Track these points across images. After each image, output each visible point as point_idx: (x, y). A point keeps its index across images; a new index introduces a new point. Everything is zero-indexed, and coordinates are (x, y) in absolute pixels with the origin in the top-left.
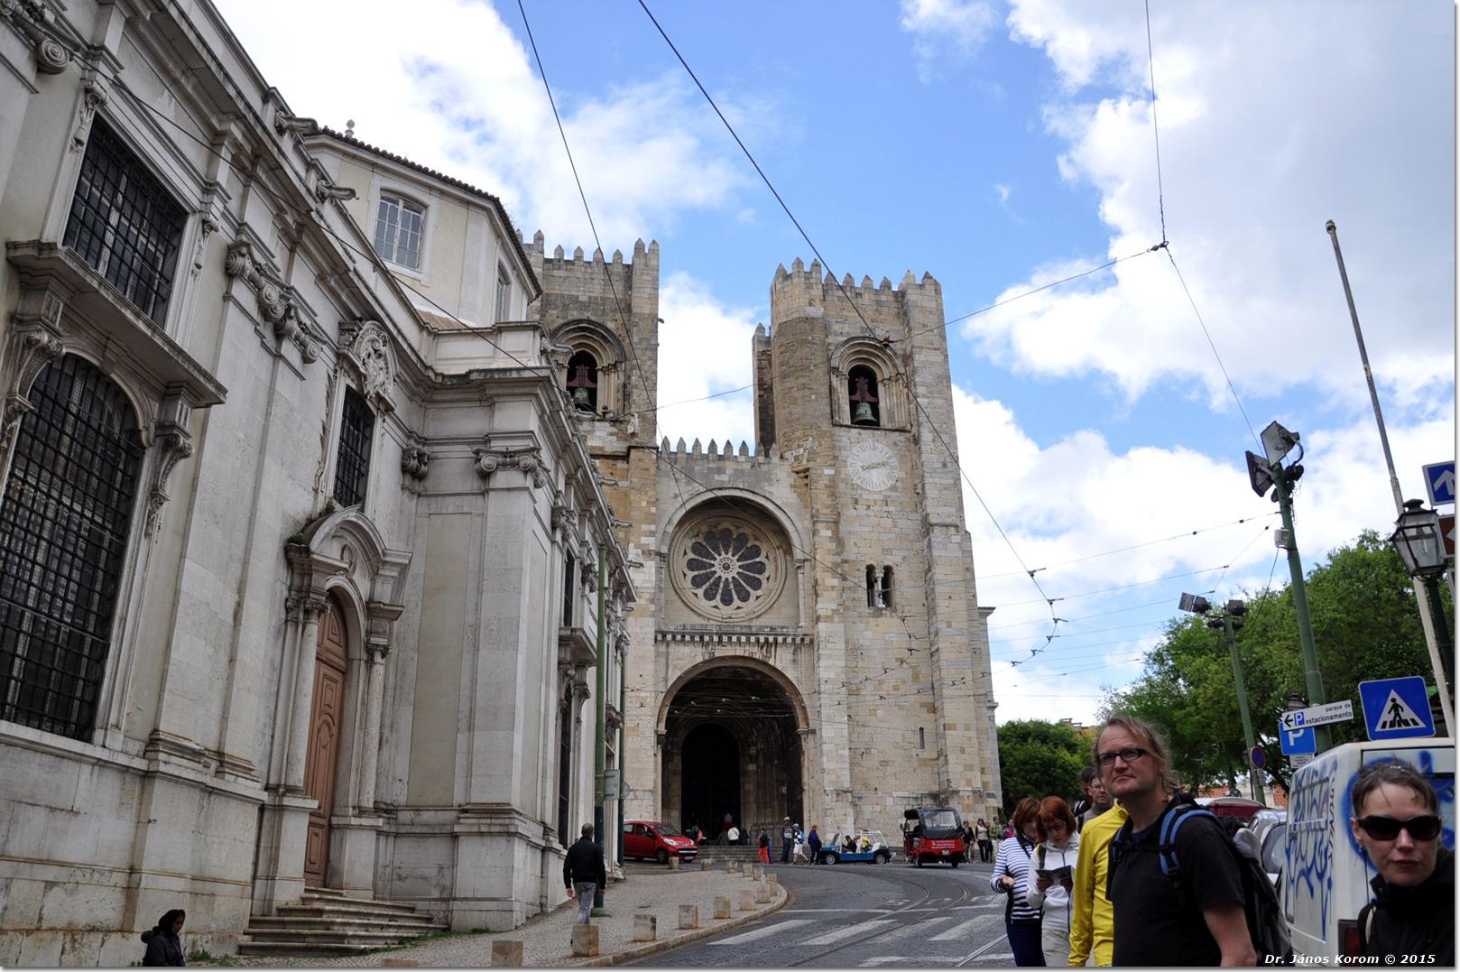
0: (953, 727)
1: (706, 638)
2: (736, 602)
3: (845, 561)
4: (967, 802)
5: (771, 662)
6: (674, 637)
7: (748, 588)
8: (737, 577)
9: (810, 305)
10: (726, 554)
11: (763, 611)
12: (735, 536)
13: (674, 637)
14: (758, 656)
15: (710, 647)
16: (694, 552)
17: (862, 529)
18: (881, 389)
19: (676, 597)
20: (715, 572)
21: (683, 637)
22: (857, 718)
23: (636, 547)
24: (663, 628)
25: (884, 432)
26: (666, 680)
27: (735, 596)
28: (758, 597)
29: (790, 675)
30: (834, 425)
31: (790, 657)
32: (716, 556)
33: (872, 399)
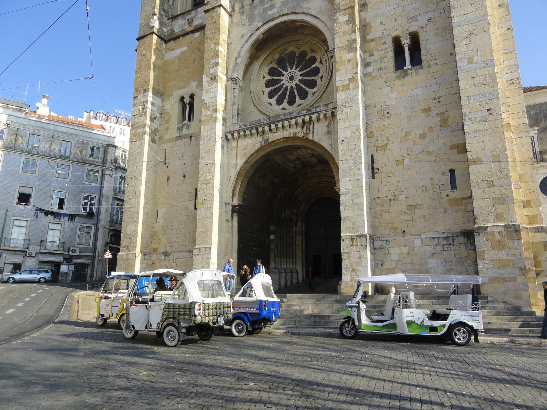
0: (476, 161)
1: (260, 129)
2: (298, 101)
3: (372, 40)
4: (498, 237)
5: (310, 137)
6: (239, 133)
7: (307, 89)
8: (298, 83)
10: (291, 69)
11: (315, 101)
12: (297, 55)
13: (239, 133)
14: (300, 134)
15: (265, 135)
16: (270, 74)
19: (254, 109)
20: (283, 84)
21: (245, 132)
22: (384, 170)
24: (232, 129)
27: (297, 97)
28: (314, 94)
29: (325, 144)
31: (325, 129)
32: (284, 73)
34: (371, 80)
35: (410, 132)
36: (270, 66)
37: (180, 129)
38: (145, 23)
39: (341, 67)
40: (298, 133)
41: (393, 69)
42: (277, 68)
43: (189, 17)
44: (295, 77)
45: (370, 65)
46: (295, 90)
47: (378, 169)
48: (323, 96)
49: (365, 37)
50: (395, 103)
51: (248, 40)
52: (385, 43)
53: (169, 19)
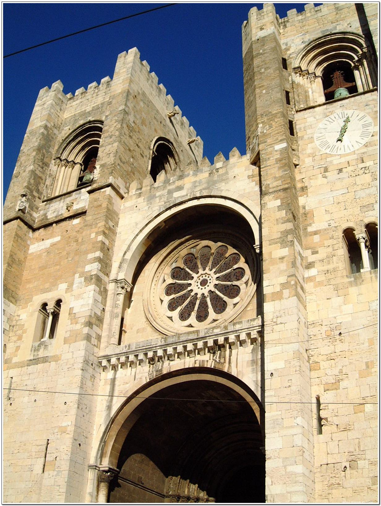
3: (315, 233)
7: (225, 298)
8: (213, 289)
9: (262, 29)
10: (204, 270)
12: (213, 251)
14: (210, 364)
16: (173, 277)
17: (334, 193)
18: (356, 73)
20: (192, 290)
21: (128, 357)
22: (336, 420)
23: (80, 277)
24: (108, 352)
25: (352, 99)
26: (109, 408)
27: (211, 310)
28: (235, 305)
30: (297, 112)
32: (194, 275)
33: (350, 85)
34: (315, 286)
35: (372, 362)
36: (174, 265)
37: (36, 349)
38: (11, 206)
39: (271, 268)
40: (207, 361)
41: (345, 273)
42: (182, 269)
43: (68, 200)
44: (209, 281)
45: (314, 267)
46: (208, 300)
47: (326, 419)
48: (248, 309)
49: (306, 229)
50: (350, 319)
51: (143, 228)
52: (332, 238)
53: (43, 202)
